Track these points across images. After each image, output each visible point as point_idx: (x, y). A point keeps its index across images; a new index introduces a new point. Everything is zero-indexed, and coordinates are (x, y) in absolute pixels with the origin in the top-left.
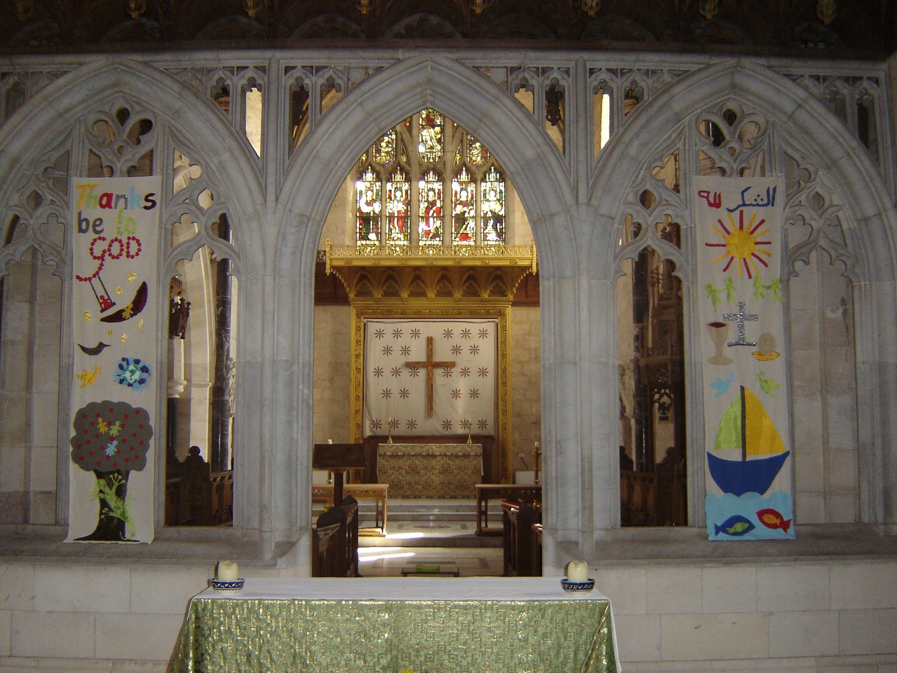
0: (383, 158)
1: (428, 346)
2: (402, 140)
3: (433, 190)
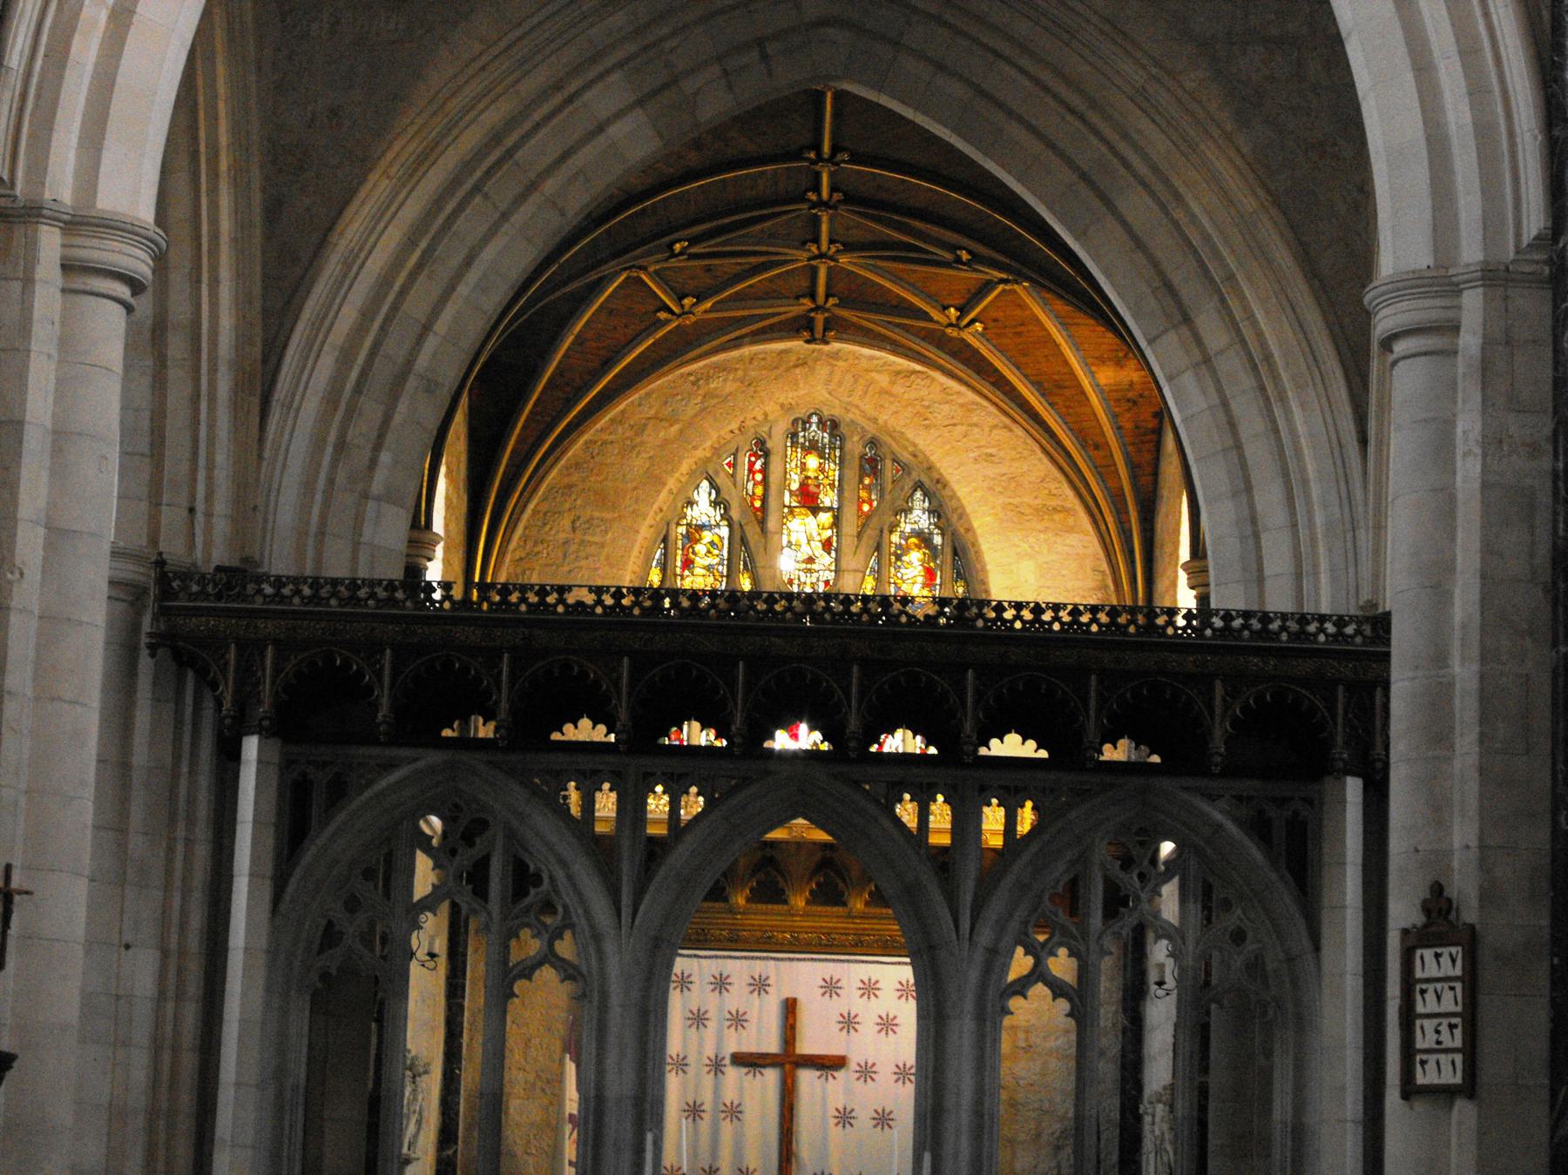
1: (787, 1018)
2: (744, 541)
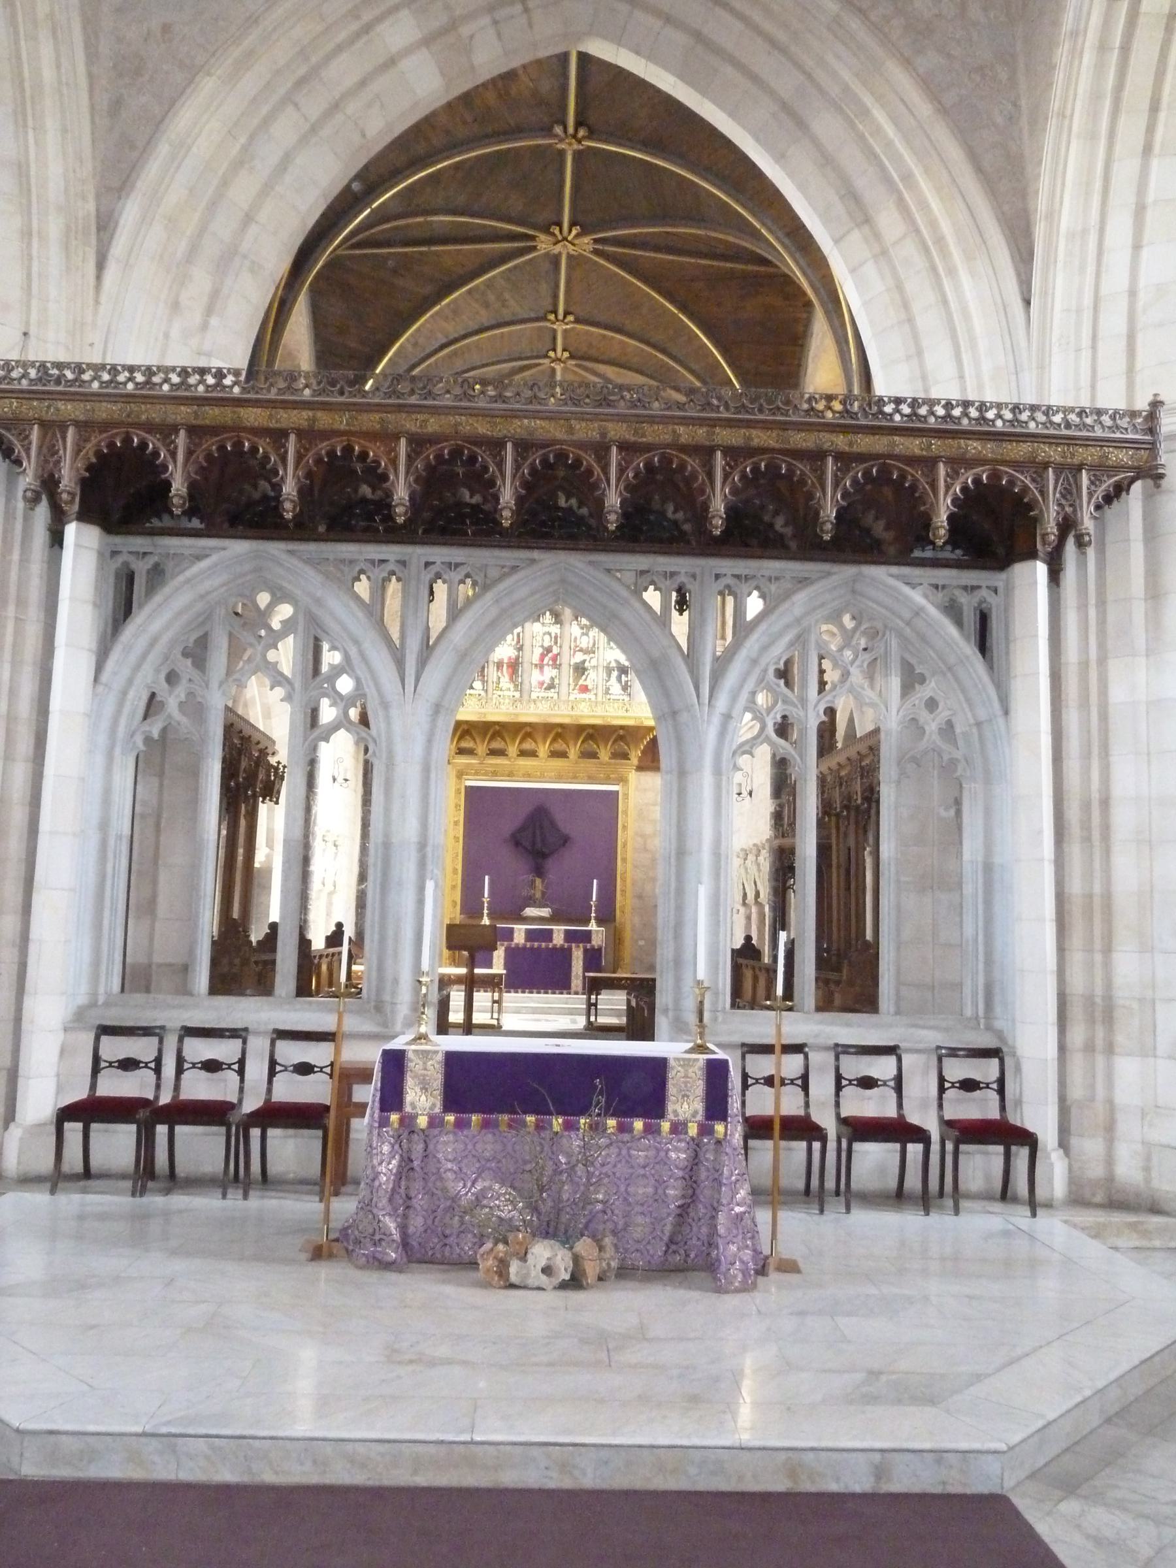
3: (550, 634)
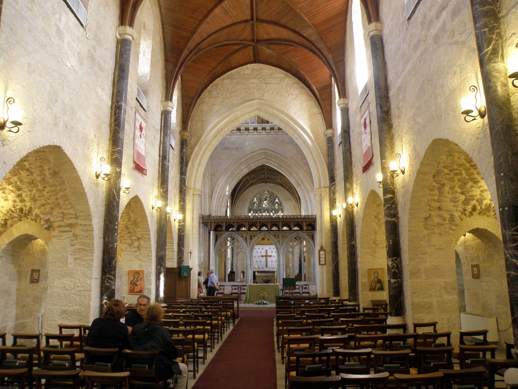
0: (255, 208)
